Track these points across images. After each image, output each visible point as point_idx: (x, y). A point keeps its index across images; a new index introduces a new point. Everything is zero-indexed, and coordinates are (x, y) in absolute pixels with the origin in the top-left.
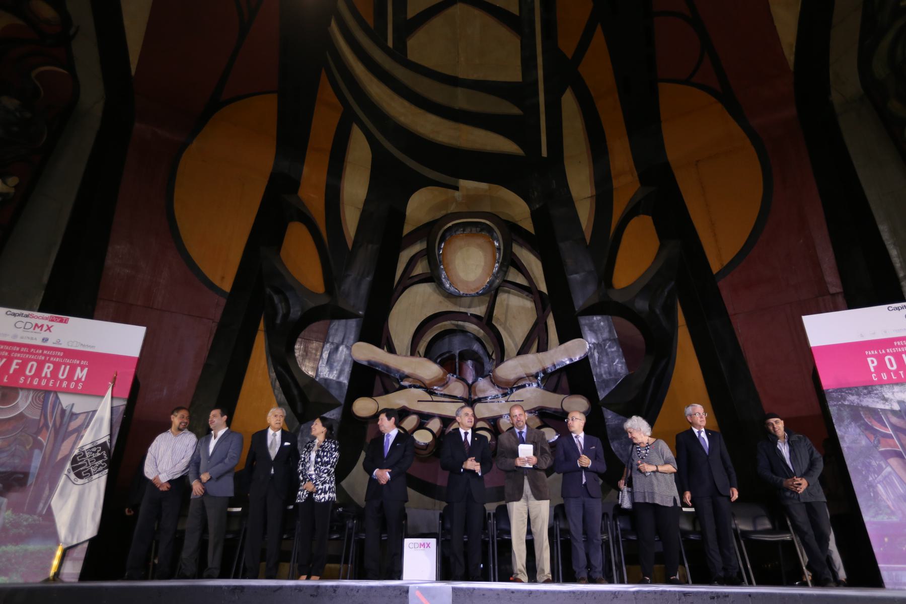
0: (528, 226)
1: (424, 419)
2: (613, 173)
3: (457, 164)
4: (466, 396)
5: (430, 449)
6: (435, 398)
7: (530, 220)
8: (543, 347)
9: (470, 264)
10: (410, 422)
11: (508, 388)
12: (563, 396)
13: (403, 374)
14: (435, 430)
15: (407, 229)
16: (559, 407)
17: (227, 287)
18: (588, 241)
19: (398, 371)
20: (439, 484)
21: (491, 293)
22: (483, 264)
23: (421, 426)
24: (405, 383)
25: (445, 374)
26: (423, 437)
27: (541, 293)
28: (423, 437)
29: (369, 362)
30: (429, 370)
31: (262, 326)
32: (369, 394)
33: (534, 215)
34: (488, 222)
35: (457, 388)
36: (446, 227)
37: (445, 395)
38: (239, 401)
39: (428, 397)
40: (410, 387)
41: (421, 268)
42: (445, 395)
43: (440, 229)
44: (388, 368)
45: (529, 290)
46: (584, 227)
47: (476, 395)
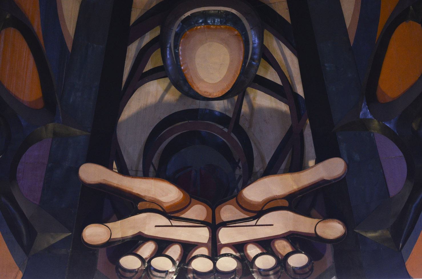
1: (162, 246)
4: (210, 221)
8: (297, 166)
11: (256, 212)
12: (316, 221)
15: (134, 16)
16: (313, 232)
18: (352, 41)
21: (237, 90)
22: (227, 62)
24: (141, 205)
27: (297, 95)
30: (168, 193)
32: (102, 220)
34: (234, 11)
35: (198, 211)
36: (183, 17)
43: (177, 18)
46: (348, 23)
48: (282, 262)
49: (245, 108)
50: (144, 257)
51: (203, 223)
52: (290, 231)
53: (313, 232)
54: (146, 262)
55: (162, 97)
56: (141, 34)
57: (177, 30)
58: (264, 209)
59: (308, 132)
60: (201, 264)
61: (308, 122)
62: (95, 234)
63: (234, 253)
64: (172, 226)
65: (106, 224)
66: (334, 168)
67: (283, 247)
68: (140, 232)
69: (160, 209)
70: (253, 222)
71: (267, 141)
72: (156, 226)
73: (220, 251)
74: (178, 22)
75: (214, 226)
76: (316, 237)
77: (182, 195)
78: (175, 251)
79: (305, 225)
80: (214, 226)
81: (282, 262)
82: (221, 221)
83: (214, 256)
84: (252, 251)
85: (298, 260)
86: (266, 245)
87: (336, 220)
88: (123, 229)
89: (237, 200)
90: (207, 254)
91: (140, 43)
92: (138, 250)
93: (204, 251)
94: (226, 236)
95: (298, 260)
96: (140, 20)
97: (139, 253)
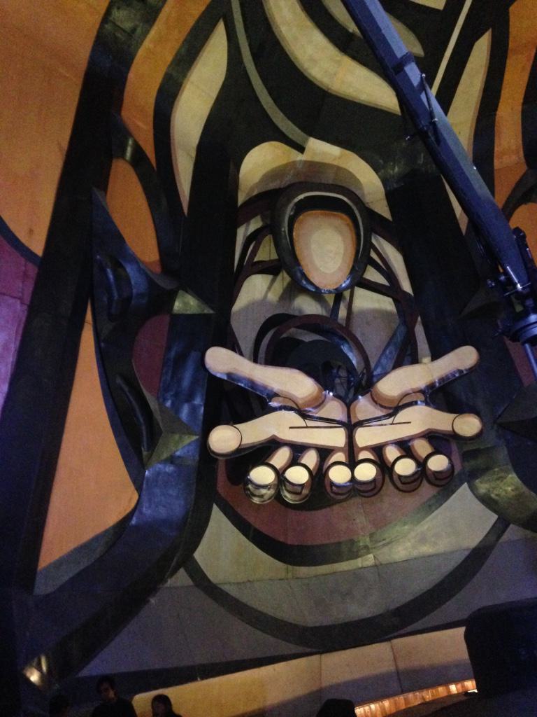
0: (383, 210)
1: (298, 450)
2: (496, 149)
3: (322, 112)
5: (305, 492)
6: (310, 423)
7: (385, 203)
9: (326, 251)
10: (281, 457)
11: (393, 409)
13: (272, 391)
14: (311, 467)
15: (241, 198)
16: (450, 429)
17: (37, 246)
19: (265, 388)
20: (289, 542)
22: (342, 251)
23: (294, 462)
24: (274, 404)
25: (320, 391)
26: (298, 475)
28: (298, 475)
29: (229, 375)
31: (89, 316)
33: (390, 196)
34: (345, 199)
35: (334, 409)
36: (296, 200)
37: (321, 419)
38: (65, 437)
39: (299, 421)
40: (280, 408)
41: (266, 252)
42: (321, 419)
43: (289, 201)
44: (252, 383)
45: (391, 290)
47: (356, 417)
48: (422, 464)
49: (343, 313)
50: (278, 467)
51: (341, 424)
52: (429, 429)
53: (451, 429)
54: (280, 474)
55: (266, 296)
56: (247, 220)
57: (292, 213)
58: (401, 404)
59: (419, 331)
60: (339, 475)
61: (419, 319)
62: (224, 439)
63: (372, 458)
64: (307, 427)
65: (237, 426)
66: (464, 357)
67: (422, 448)
68: (274, 436)
69: (295, 406)
70: (390, 420)
71: (375, 340)
72: (291, 428)
73: (358, 456)
74: (291, 205)
75: (351, 427)
76: (454, 436)
77: (317, 389)
78: (311, 459)
79: (442, 421)
80: (351, 427)
81: (422, 464)
82: (356, 421)
83: (352, 463)
84: (392, 453)
85: (438, 463)
86: (405, 446)
87: (472, 415)
88: (255, 431)
89: (371, 395)
90: (344, 461)
91: (246, 230)
92: (270, 460)
93: (340, 456)
94: (365, 437)
95: (438, 463)
96: (246, 204)
97: (272, 462)
